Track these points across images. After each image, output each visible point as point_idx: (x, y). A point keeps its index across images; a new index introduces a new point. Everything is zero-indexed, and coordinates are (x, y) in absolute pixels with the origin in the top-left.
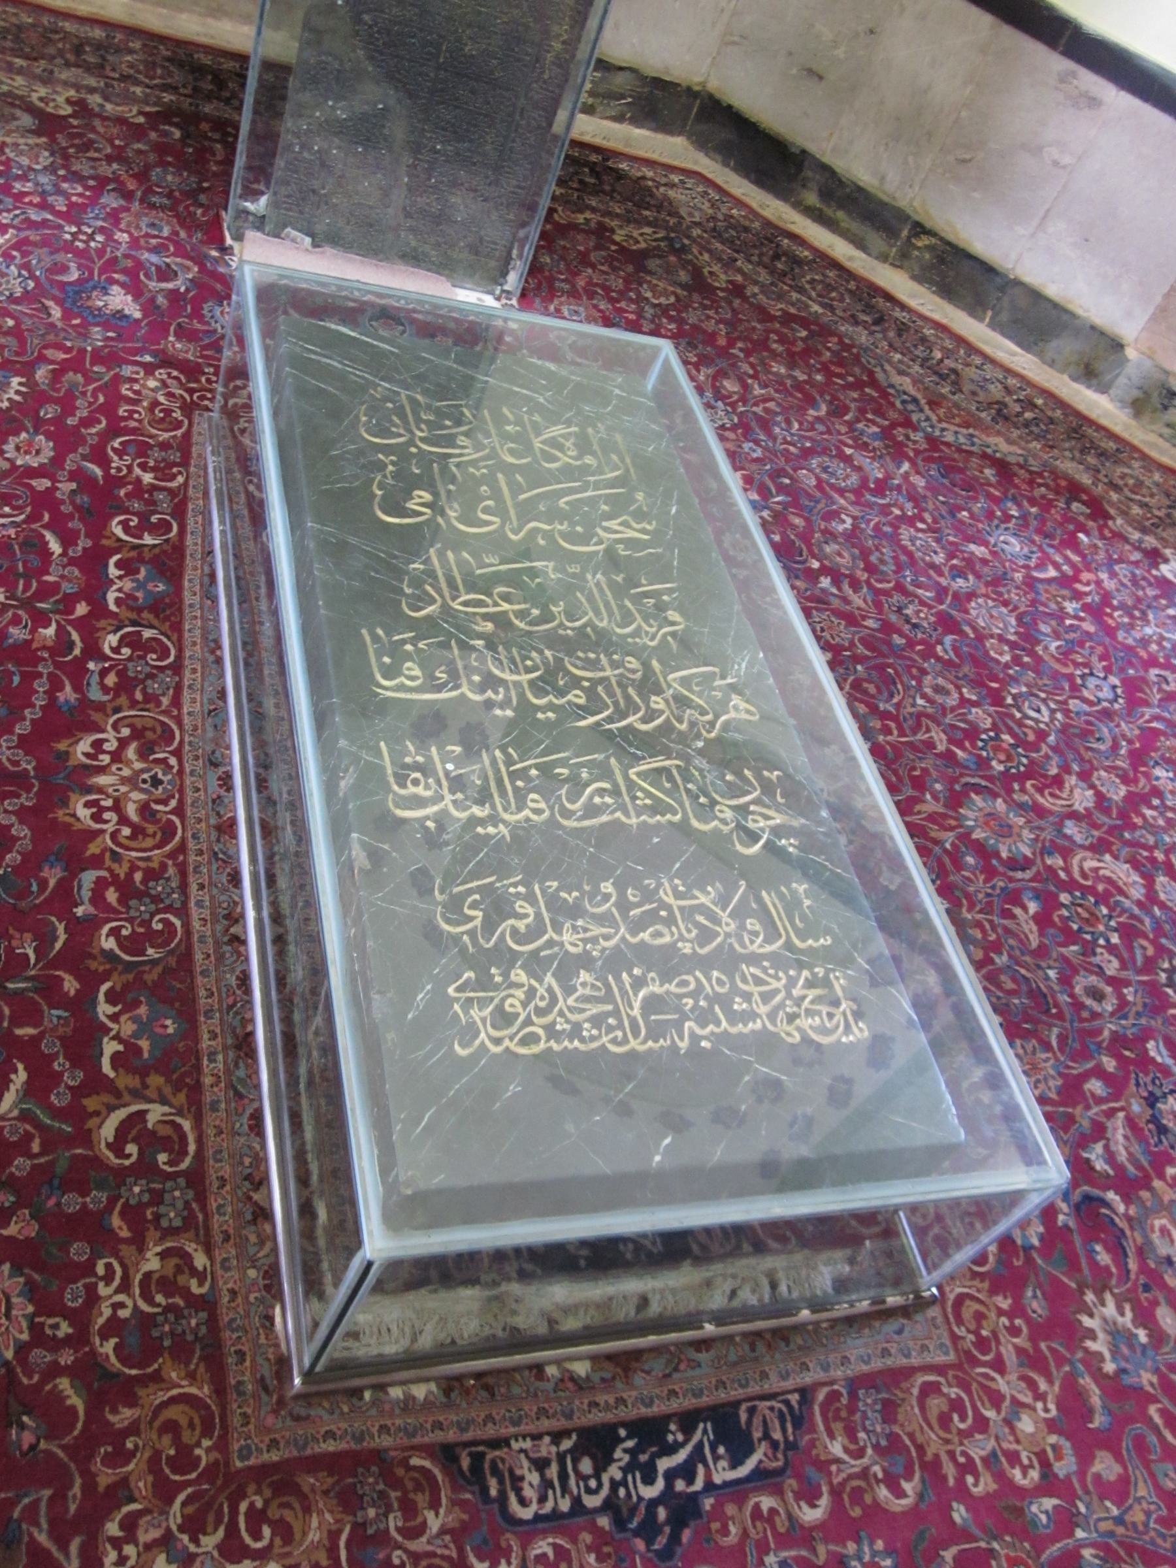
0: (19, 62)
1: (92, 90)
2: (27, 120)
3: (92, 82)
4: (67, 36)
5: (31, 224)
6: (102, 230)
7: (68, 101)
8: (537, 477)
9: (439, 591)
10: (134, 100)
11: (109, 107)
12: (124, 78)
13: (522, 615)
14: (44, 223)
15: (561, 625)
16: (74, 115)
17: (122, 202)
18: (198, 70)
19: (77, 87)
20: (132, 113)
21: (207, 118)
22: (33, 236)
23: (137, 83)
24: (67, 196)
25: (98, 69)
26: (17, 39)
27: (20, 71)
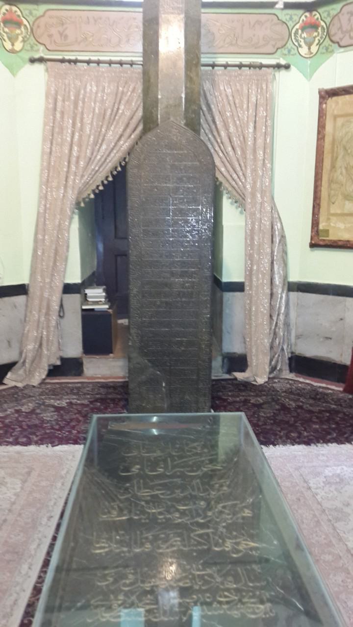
0: (52, 397)
1: (73, 399)
2: (52, 409)
3: (75, 397)
4: (69, 387)
5: (46, 433)
6: (68, 431)
7: (67, 403)
8: (181, 457)
9: (133, 491)
10: (87, 398)
11: (79, 402)
12: (85, 394)
13: (162, 494)
14: (51, 433)
15: (179, 495)
16: (67, 406)
17: (77, 423)
18: (110, 387)
19: (69, 399)
20: (86, 402)
21: (109, 399)
22: (46, 436)
23: (88, 394)
24: (59, 425)
25: (77, 394)
26: (54, 391)
27: (53, 399)
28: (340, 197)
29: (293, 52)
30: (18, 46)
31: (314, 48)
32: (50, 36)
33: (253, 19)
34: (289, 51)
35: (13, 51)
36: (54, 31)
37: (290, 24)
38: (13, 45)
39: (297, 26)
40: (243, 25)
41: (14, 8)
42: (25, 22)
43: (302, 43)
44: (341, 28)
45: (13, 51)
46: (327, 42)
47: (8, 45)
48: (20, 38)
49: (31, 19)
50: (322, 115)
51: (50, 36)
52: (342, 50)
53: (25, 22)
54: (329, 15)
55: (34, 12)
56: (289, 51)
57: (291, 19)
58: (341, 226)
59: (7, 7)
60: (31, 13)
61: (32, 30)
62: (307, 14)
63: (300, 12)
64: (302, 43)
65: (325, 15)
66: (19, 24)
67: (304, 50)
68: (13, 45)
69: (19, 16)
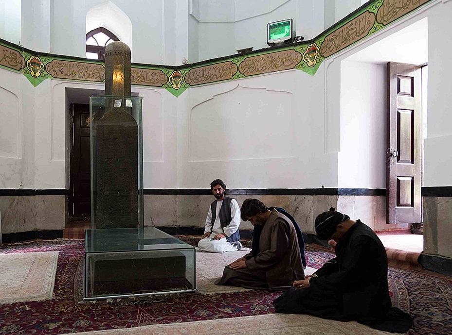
29: (170, 86)
30: (38, 74)
31: (179, 86)
34: (168, 86)
35: (34, 76)
36: (57, 69)
37: (168, 75)
38: (35, 74)
39: (171, 76)
40: (147, 74)
42: (42, 64)
44: (190, 78)
47: (33, 74)
48: (39, 71)
52: (191, 87)
53: (42, 64)
54: (184, 72)
55: (47, 60)
56: (168, 86)
57: (168, 73)
59: (33, 57)
60: (45, 60)
61: (45, 68)
62: (175, 71)
63: (172, 70)
65: (183, 72)
66: (39, 65)
67: (175, 86)
68: (35, 74)
69: (39, 61)
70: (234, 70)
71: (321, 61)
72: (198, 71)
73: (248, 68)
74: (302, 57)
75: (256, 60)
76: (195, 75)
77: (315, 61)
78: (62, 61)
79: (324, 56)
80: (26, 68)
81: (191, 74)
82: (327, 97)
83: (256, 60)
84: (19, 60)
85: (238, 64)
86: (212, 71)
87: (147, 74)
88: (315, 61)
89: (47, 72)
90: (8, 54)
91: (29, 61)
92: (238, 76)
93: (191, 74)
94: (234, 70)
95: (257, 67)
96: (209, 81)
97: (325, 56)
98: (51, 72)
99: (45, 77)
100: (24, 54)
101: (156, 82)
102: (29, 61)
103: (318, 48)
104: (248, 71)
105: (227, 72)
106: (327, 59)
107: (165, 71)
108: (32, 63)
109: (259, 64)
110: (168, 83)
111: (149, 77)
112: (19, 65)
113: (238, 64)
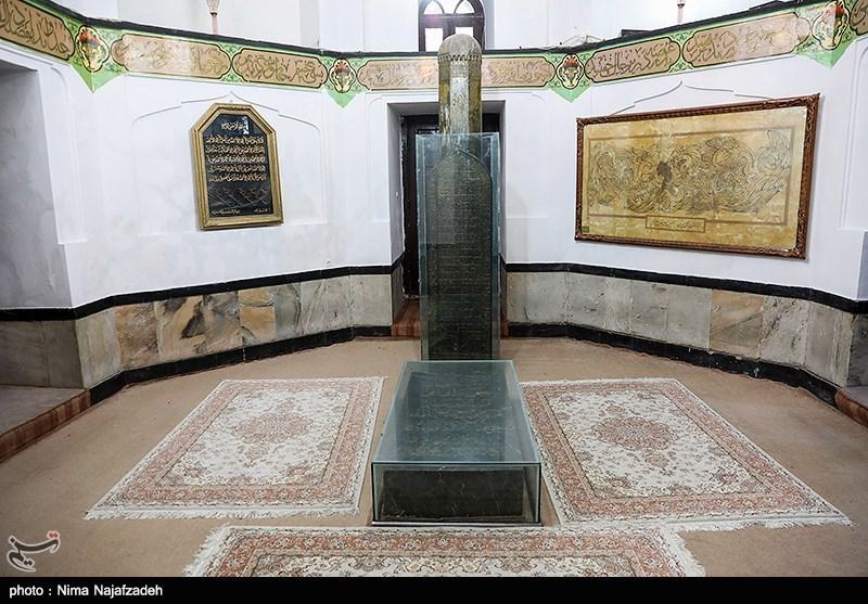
28: (596, 201)
30: (346, 88)
31: (575, 82)
32: (370, 79)
33: (526, 61)
36: (373, 76)
37: (556, 64)
40: (519, 66)
41: (344, 61)
43: (565, 78)
45: (341, 92)
46: (584, 78)
49: (356, 68)
50: (580, 138)
51: (370, 79)
58: (597, 223)
64: (565, 78)
70: (674, 56)
71: (849, 40)
72: (608, 57)
73: (701, 51)
74: (811, 29)
75: (716, 35)
76: (603, 63)
77: (838, 38)
78: (380, 62)
79: (856, 30)
80: (329, 82)
81: (596, 62)
82: (854, 123)
83: (716, 35)
84: (317, 71)
85: (681, 43)
86: (633, 56)
87: (519, 66)
88: (838, 38)
89: (359, 82)
90: (301, 66)
91: (333, 70)
92: (680, 67)
93: (596, 62)
94: (674, 56)
95: (717, 50)
96: (627, 74)
97: (859, 31)
98: (367, 82)
99: (358, 90)
100: (325, 60)
101: (534, 78)
102: (333, 70)
103: (846, 11)
104: (701, 57)
105: (662, 58)
106: (862, 37)
107: (549, 57)
108: (338, 71)
109: (721, 43)
110: (556, 79)
111: (523, 72)
112: (319, 80)
113: (681, 43)
